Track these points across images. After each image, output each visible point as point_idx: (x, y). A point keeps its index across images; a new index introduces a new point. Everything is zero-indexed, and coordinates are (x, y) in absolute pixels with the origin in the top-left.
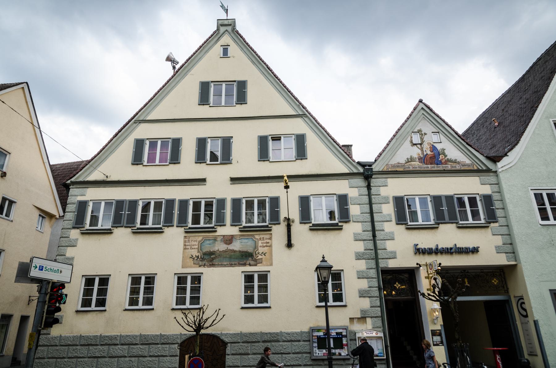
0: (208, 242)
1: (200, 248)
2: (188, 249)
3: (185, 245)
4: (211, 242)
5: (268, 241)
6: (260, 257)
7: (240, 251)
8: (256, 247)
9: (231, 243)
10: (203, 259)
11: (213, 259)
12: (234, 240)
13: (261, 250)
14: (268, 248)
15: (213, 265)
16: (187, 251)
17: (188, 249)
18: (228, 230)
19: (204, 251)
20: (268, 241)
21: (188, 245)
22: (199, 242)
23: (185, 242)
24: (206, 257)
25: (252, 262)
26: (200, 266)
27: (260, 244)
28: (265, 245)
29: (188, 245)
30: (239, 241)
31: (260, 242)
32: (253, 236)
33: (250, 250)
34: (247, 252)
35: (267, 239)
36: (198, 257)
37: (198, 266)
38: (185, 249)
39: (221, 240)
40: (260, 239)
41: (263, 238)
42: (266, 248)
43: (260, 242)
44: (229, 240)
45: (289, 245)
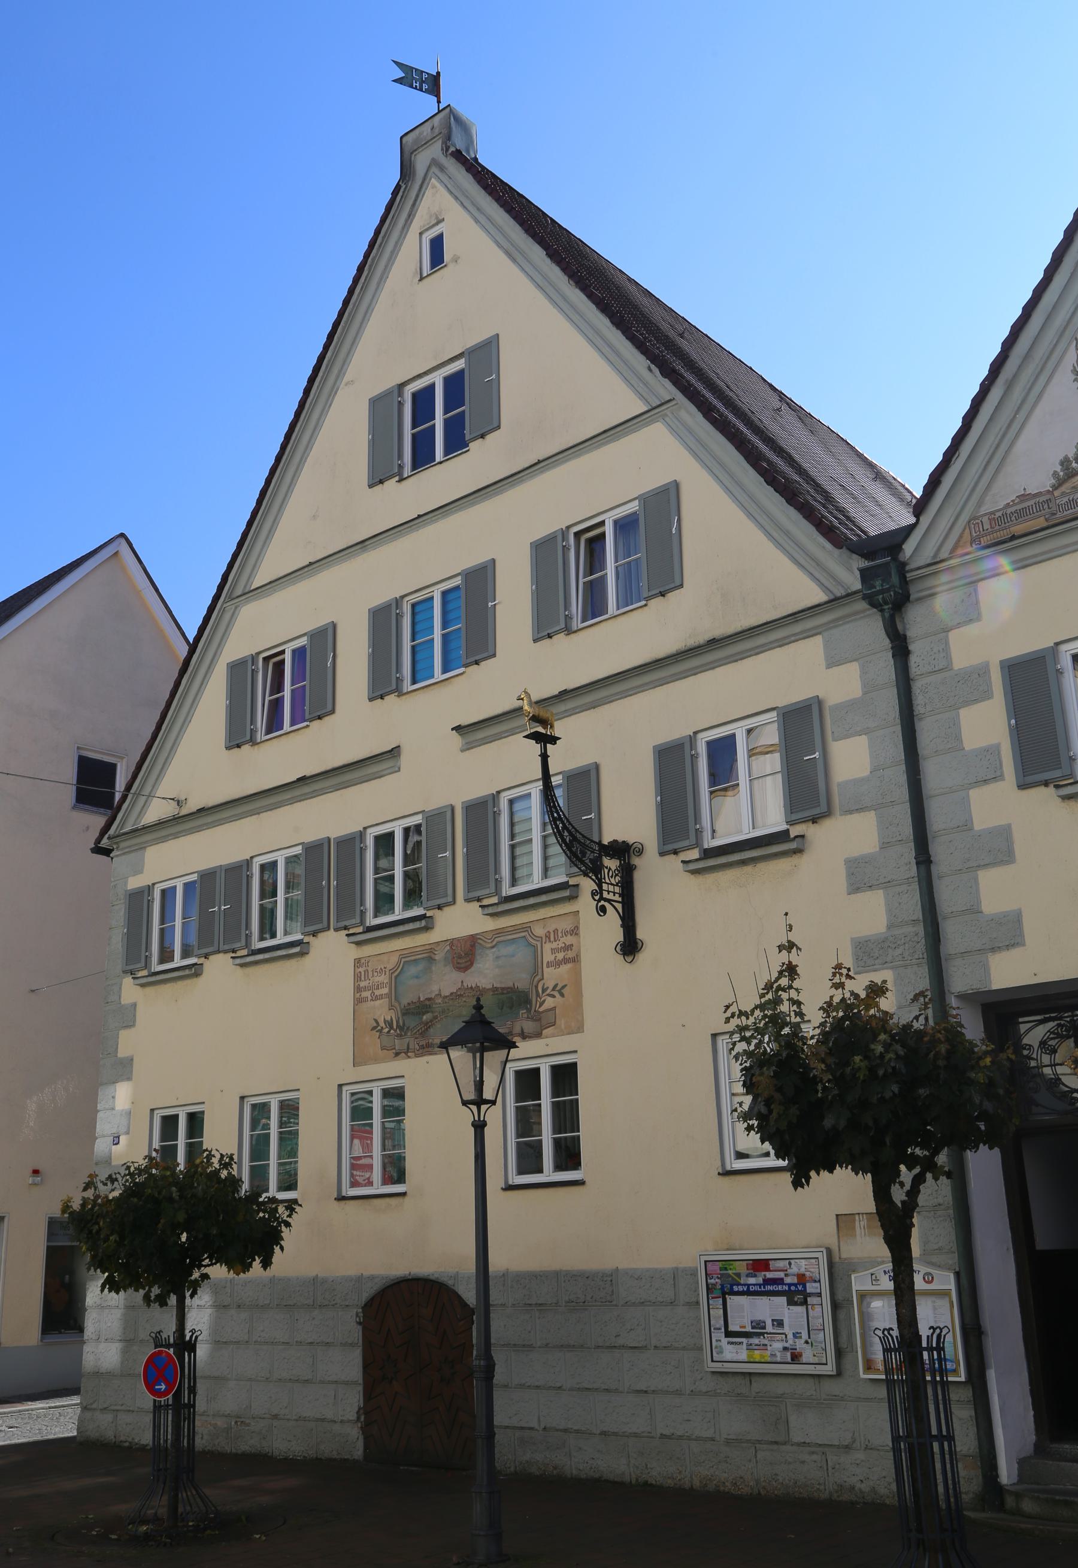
0: (413, 970)
1: (394, 996)
2: (365, 1000)
3: (358, 989)
4: (421, 967)
5: (569, 940)
6: (549, 1003)
7: (495, 990)
8: (536, 970)
9: (472, 964)
10: (403, 1030)
11: (428, 1025)
12: (478, 951)
13: (551, 976)
14: (569, 966)
15: (429, 1045)
16: (364, 1006)
17: (365, 1000)
18: (460, 920)
19: (405, 1001)
20: (569, 940)
21: (365, 989)
22: (392, 971)
23: (357, 977)
24: (411, 1022)
25: (529, 1026)
26: (397, 1054)
27: (548, 957)
28: (560, 956)
29: (365, 989)
30: (491, 954)
31: (547, 947)
32: (526, 928)
33: (521, 982)
34: (511, 990)
35: (566, 933)
36: (389, 1024)
37: (391, 1053)
38: (358, 1001)
39: (446, 959)
40: (548, 936)
41: (556, 931)
42: (565, 968)
43: (547, 947)
44: (465, 952)
45: (630, 946)
